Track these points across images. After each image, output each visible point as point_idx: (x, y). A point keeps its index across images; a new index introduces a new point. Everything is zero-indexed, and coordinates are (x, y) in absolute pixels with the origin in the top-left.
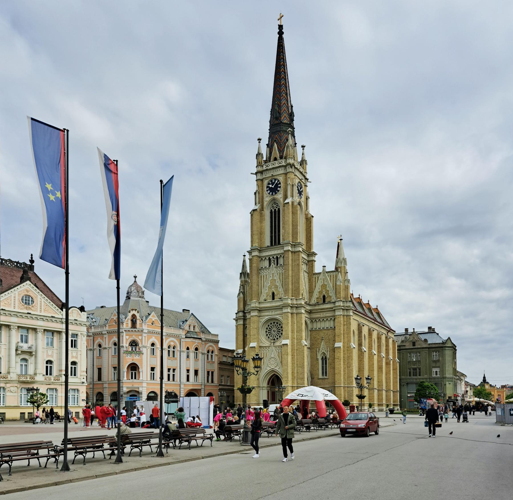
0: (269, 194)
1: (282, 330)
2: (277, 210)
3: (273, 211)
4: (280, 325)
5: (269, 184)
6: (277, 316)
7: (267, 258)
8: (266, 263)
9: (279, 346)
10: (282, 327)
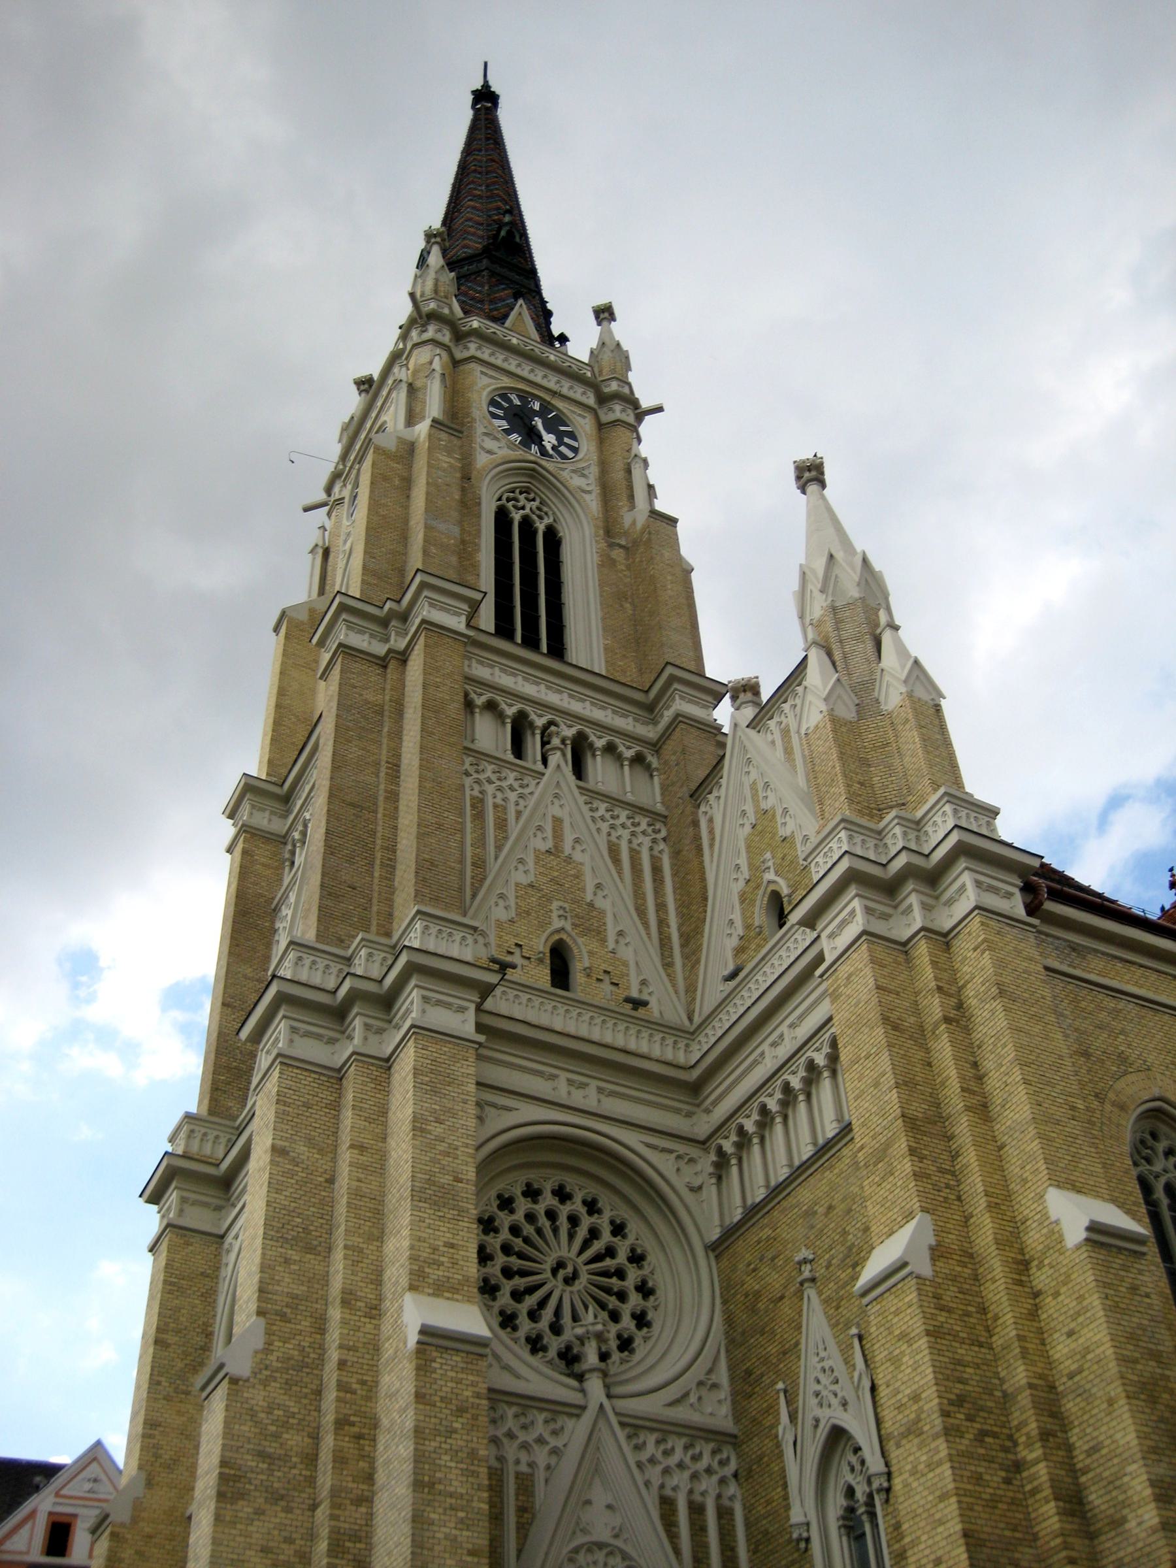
2: (541, 527)
3: (517, 517)
4: (618, 1229)
7: (510, 711)
8: (490, 736)
9: (665, 1429)
10: (637, 1258)
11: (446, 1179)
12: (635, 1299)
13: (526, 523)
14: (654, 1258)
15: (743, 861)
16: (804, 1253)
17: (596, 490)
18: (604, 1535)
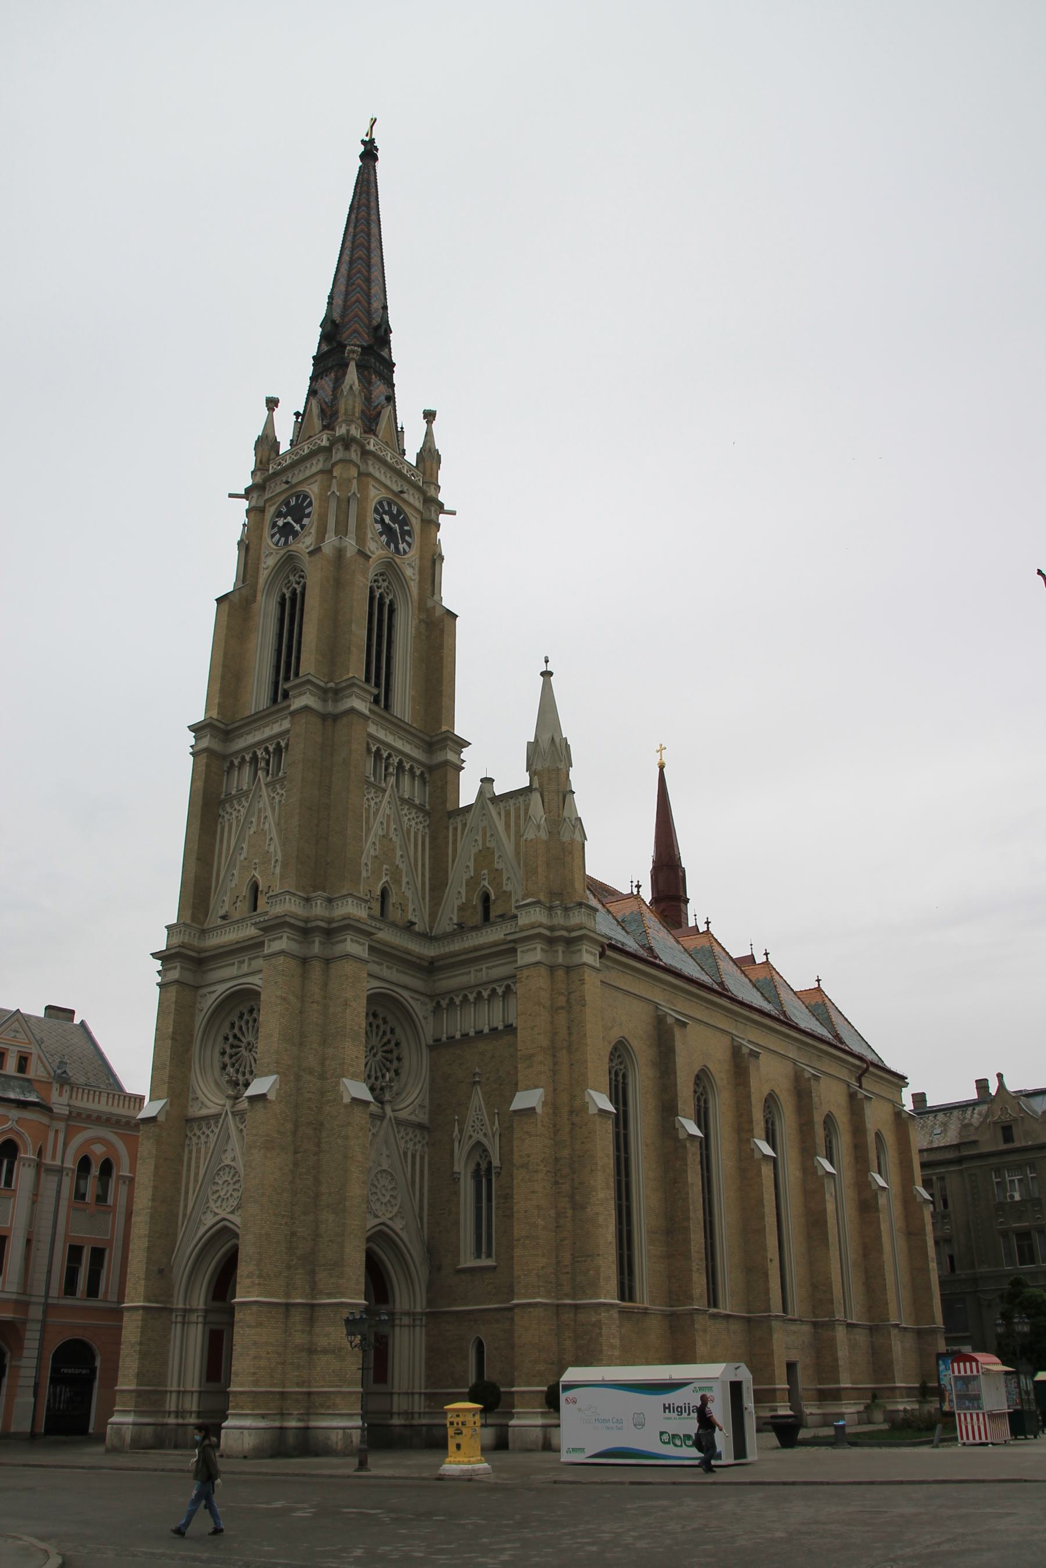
0: (381, 534)
1: (399, 1059)
4: (392, 1031)
5: (380, 503)
6: (406, 994)
10: (397, 1044)
11: (356, 1028)
12: (395, 1064)
13: (381, 596)
14: (404, 1044)
15: (472, 865)
16: (477, 1070)
17: (416, 577)
18: (385, 1167)
